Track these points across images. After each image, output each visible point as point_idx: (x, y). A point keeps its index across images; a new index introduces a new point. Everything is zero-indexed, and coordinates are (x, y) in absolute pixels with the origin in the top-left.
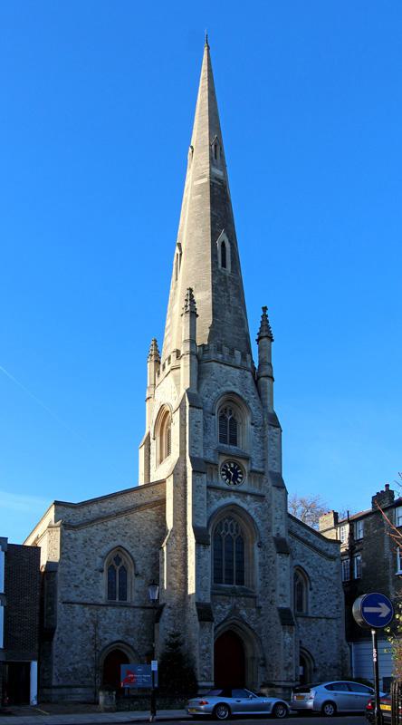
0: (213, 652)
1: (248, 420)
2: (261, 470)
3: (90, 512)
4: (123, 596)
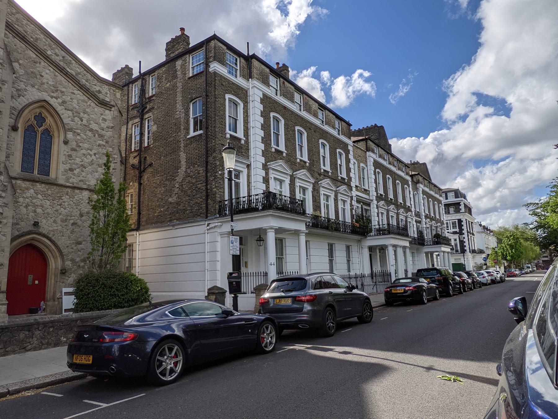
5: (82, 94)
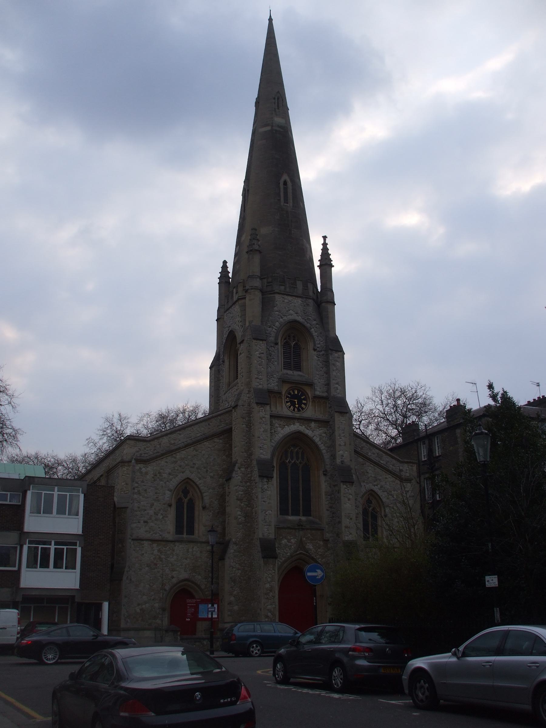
0: (277, 592)
1: (311, 346)
2: (325, 394)
3: (160, 444)
4: (191, 531)
5: (392, 477)
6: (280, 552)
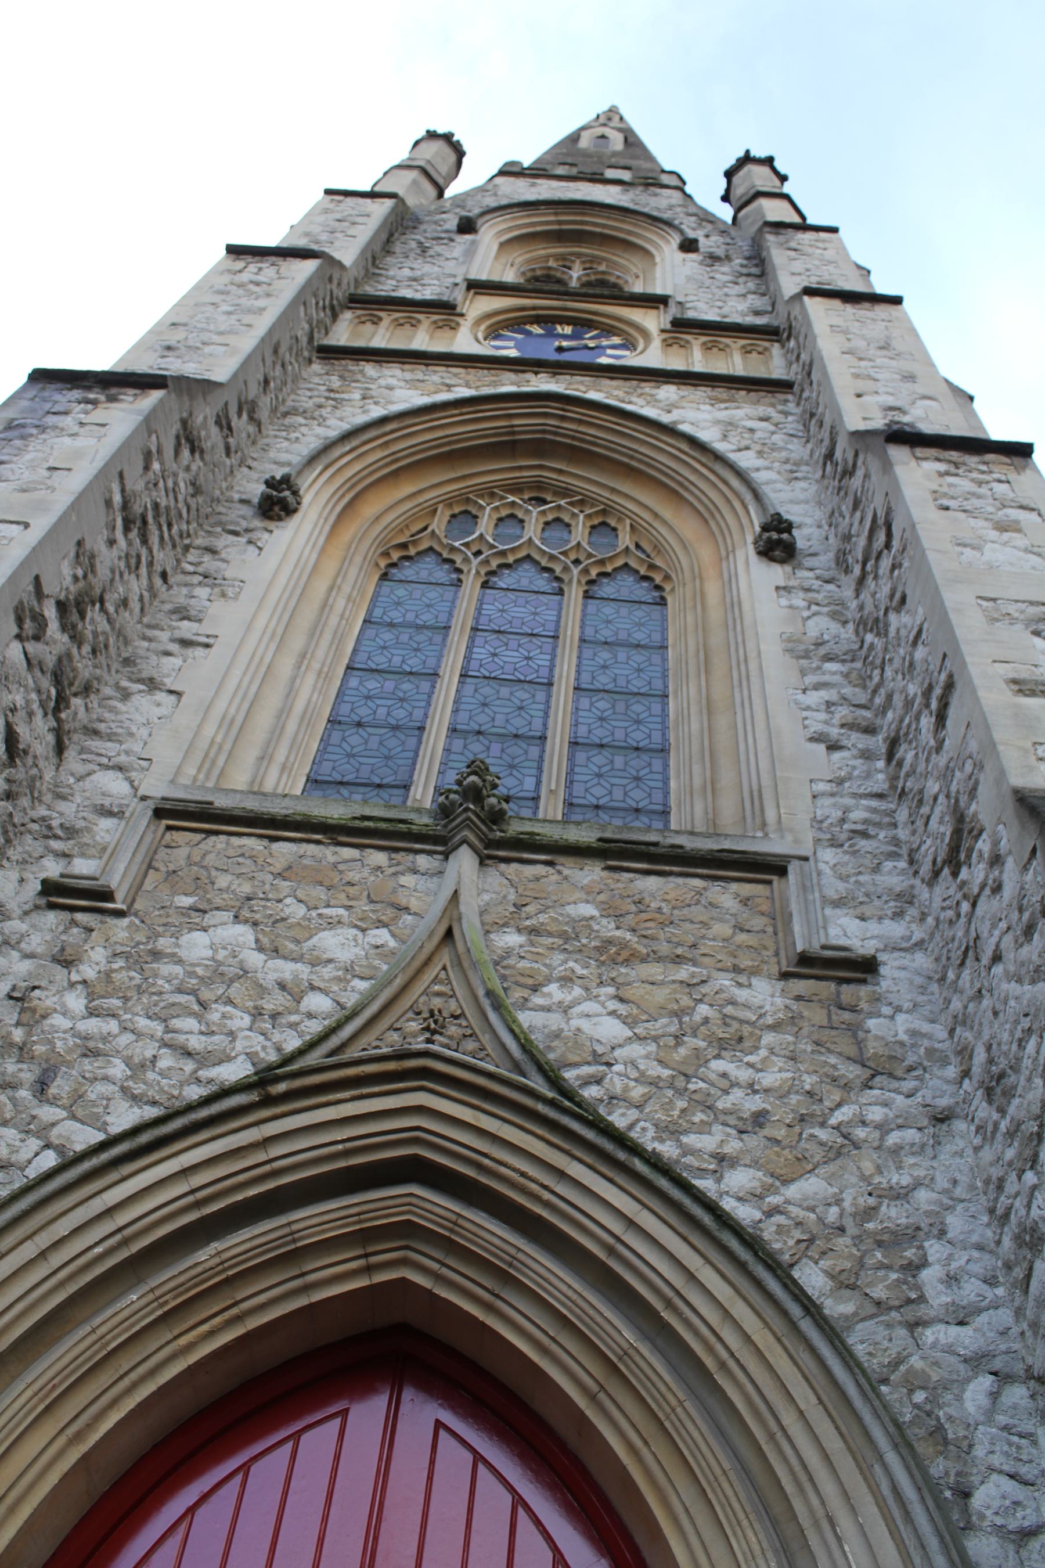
6: (105, 1038)
